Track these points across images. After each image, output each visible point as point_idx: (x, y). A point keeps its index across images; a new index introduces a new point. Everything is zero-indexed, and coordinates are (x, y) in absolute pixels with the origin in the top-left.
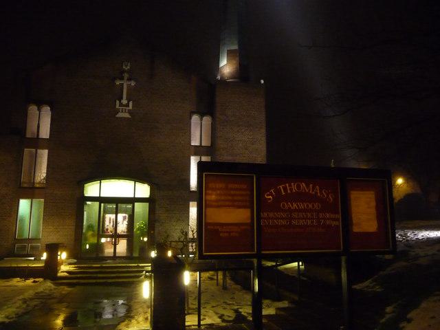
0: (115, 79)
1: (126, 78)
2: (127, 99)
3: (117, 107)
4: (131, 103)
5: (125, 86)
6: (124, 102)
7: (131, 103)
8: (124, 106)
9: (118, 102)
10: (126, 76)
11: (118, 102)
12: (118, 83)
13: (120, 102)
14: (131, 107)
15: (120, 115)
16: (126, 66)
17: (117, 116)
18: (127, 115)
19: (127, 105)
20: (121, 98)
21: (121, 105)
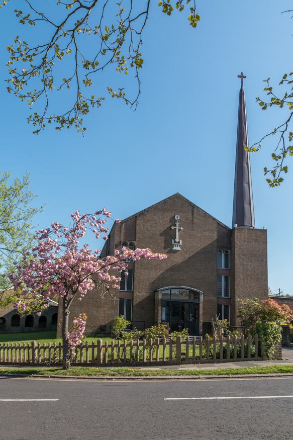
0: (171, 226)
1: (177, 225)
3: (173, 243)
4: (181, 241)
6: (177, 240)
7: (181, 241)
9: (173, 240)
10: (177, 224)
11: (173, 240)
12: (173, 228)
14: (181, 244)
15: (175, 248)
16: (177, 217)
17: (173, 249)
18: (178, 248)
19: (179, 242)
20: (176, 238)
21: (175, 242)
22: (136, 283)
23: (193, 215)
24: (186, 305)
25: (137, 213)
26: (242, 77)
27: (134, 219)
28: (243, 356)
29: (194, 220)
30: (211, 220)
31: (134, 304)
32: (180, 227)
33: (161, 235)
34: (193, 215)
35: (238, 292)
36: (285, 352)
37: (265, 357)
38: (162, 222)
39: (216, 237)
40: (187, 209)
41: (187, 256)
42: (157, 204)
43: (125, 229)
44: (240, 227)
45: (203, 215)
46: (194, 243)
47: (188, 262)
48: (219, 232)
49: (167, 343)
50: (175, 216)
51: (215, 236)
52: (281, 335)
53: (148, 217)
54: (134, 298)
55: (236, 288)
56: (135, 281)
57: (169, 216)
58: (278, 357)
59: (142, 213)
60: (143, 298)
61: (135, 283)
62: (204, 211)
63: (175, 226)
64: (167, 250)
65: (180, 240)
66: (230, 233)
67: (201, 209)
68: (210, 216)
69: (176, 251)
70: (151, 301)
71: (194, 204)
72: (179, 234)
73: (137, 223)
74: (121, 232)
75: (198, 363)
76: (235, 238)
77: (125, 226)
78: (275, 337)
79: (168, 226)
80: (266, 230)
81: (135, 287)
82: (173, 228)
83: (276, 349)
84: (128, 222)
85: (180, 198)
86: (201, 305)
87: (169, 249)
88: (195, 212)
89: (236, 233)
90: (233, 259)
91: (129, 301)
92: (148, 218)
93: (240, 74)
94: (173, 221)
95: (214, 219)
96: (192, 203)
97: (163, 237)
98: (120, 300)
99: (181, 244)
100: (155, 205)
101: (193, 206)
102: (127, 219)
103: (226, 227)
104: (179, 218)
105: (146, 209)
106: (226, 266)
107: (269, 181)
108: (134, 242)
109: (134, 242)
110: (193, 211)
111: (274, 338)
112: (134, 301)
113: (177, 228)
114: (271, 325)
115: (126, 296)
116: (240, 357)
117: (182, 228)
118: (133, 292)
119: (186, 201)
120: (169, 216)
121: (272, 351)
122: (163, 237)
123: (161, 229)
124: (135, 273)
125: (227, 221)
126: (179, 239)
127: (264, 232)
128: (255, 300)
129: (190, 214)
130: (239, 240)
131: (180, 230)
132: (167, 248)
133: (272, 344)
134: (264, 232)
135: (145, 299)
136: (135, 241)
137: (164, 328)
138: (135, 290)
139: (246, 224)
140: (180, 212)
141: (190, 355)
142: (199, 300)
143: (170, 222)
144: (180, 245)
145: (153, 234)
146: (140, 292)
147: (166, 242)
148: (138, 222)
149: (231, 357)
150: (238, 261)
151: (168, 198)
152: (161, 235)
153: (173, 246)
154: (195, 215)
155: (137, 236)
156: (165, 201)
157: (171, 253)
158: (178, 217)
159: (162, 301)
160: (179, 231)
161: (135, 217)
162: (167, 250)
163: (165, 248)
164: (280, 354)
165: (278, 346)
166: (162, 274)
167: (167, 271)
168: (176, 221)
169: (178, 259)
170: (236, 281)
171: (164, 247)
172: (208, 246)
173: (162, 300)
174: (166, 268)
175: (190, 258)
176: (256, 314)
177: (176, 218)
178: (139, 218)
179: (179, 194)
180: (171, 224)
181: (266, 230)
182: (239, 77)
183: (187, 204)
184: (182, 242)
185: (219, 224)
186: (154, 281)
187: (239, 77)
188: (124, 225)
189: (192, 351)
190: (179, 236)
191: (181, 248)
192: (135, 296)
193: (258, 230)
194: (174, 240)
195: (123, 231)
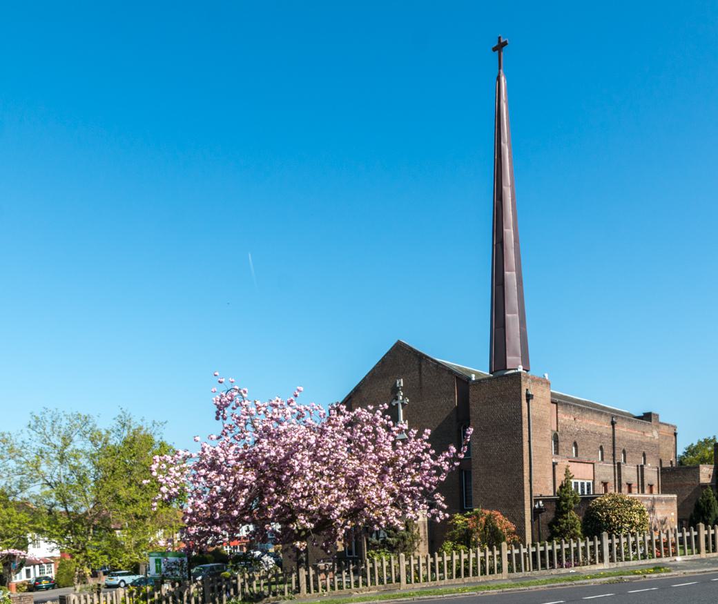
0: (392, 401)
5: (400, 406)
16: (400, 383)
23: (420, 373)
30: (445, 374)
34: (420, 373)
42: (374, 368)
45: (434, 368)
46: (424, 422)
53: (365, 394)
55: (473, 491)
63: (397, 399)
67: (432, 360)
71: (421, 354)
85: (403, 348)
88: (423, 366)
96: (418, 352)
98: (428, 521)
101: (421, 357)
105: (360, 382)
110: (420, 365)
125: (477, 365)
126: (404, 420)
131: (403, 405)
156: (383, 362)
158: (401, 383)
160: (402, 408)
172: (444, 421)
177: (398, 386)
190: (404, 416)
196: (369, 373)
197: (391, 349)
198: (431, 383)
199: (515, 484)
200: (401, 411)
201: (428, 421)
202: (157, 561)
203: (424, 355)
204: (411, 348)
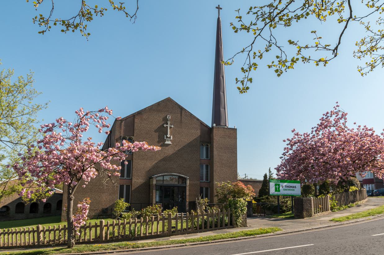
0: (164, 124)
1: (169, 124)
2: (170, 135)
3: (165, 138)
4: (172, 137)
6: (168, 136)
7: (172, 137)
8: (169, 138)
9: (165, 136)
10: (169, 123)
11: (165, 136)
12: (165, 126)
13: (166, 136)
14: (171, 139)
15: (167, 142)
16: (169, 117)
18: (170, 143)
19: (170, 138)
20: (167, 134)
21: (167, 137)
22: (134, 172)
23: (181, 116)
24: (175, 188)
25: (136, 113)
26: (219, 8)
27: (133, 117)
28: (219, 226)
29: (183, 120)
30: (195, 120)
31: (132, 189)
32: (171, 125)
33: (156, 131)
34: (181, 116)
35: (215, 177)
36: (249, 221)
37: (235, 226)
38: (156, 120)
39: (199, 134)
40: (176, 111)
41: (176, 149)
42: (152, 105)
43: (125, 126)
44: (218, 126)
47: (178, 154)
48: (201, 130)
49: (161, 220)
50: (167, 116)
51: (198, 133)
52: (246, 208)
53: (145, 116)
54: (133, 184)
55: (214, 174)
56: (133, 170)
57: (162, 115)
58: (244, 225)
59: (139, 113)
60: (140, 184)
61: (133, 172)
62: (190, 113)
63: (167, 124)
64: (160, 144)
65: (171, 136)
66: (211, 130)
68: (195, 117)
69: (168, 145)
70: (147, 186)
71: (182, 107)
72: (170, 131)
73: (135, 121)
74: (121, 128)
75: (185, 234)
76: (214, 135)
77: (125, 123)
78: (243, 210)
79: (161, 124)
80: (236, 129)
81: (133, 174)
82: (165, 126)
83: (243, 219)
84: (127, 120)
85: (171, 101)
86: (188, 188)
87: (162, 143)
88: (183, 113)
89: (215, 131)
90: (212, 151)
91: (128, 187)
92: (144, 117)
93: (218, 6)
94: (166, 120)
95: (198, 120)
96: (180, 106)
97: (157, 133)
98: (120, 186)
99: (171, 139)
100: (150, 106)
101: (182, 109)
102: (127, 117)
103: (207, 126)
104: (170, 118)
105: (142, 110)
106: (207, 157)
107: (239, 88)
108: (132, 137)
109: (132, 137)
111: (242, 210)
112: (132, 187)
113: (169, 126)
114: (240, 201)
115: (125, 183)
116: (217, 227)
117: (172, 126)
118: (131, 179)
119: (176, 105)
120: (162, 115)
121: (240, 220)
122: (157, 133)
123: (156, 126)
124: (133, 164)
126: (171, 135)
127: (235, 130)
128: (228, 183)
129: (179, 115)
130: (217, 136)
131: (171, 127)
132: (160, 142)
133: (240, 215)
134: (235, 130)
135: (142, 185)
136: (134, 136)
137: (157, 208)
138: (133, 178)
139: (222, 124)
140: (171, 113)
141: (179, 227)
142: (186, 184)
143: (163, 120)
144: (171, 140)
145: (149, 131)
146: (138, 179)
147: (159, 137)
148: (136, 120)
149: (211, 227)
150: (215, 153)
151: (161, 101)
152: (156, 131)
153: (165, 141)
154: (183, 116)
155: (135, 132)
156: (158, 104)
157: (164, 146)
158: (169, 117)
159: (156, 186)
160: (170, 129)
161: (134, 116)
162: (160, 144)
163: (159, 142)
164: (246, 222)
165: (244, 217)
166: (156, 164)
167: (160, 161)
168: (167, 120)
169: (170, 151)
170: (215, 169)
171: (158, 142)
172: (193, 140)
173: (156, 185)
174: (160, 158)
175: (179, 151)
176: (229, 194)
177: (168, 118)
178: (136, 117)
179: (171, 99)
180: (163, 122)
181: (236, 129)
182: (217, 8)
183: (177, 107)
184: (173, 137)
185: (202, 124)
186: (150, 170)
187: (217, 8)
188: (123, 122)
189: (180, 225)
190: (170, 133)
191: (172, 142)
192: (133, 182)
193: (231, 128)
194: (166, 136)
195: (123, 127)
196: (149, 107)
197: (165, 100)
198: (187, 122)
199: (233, 172)
200: (169, 130)
201: (184, 139)
202: (276, 185)
203: (184, 108)
204: (177, 104)
